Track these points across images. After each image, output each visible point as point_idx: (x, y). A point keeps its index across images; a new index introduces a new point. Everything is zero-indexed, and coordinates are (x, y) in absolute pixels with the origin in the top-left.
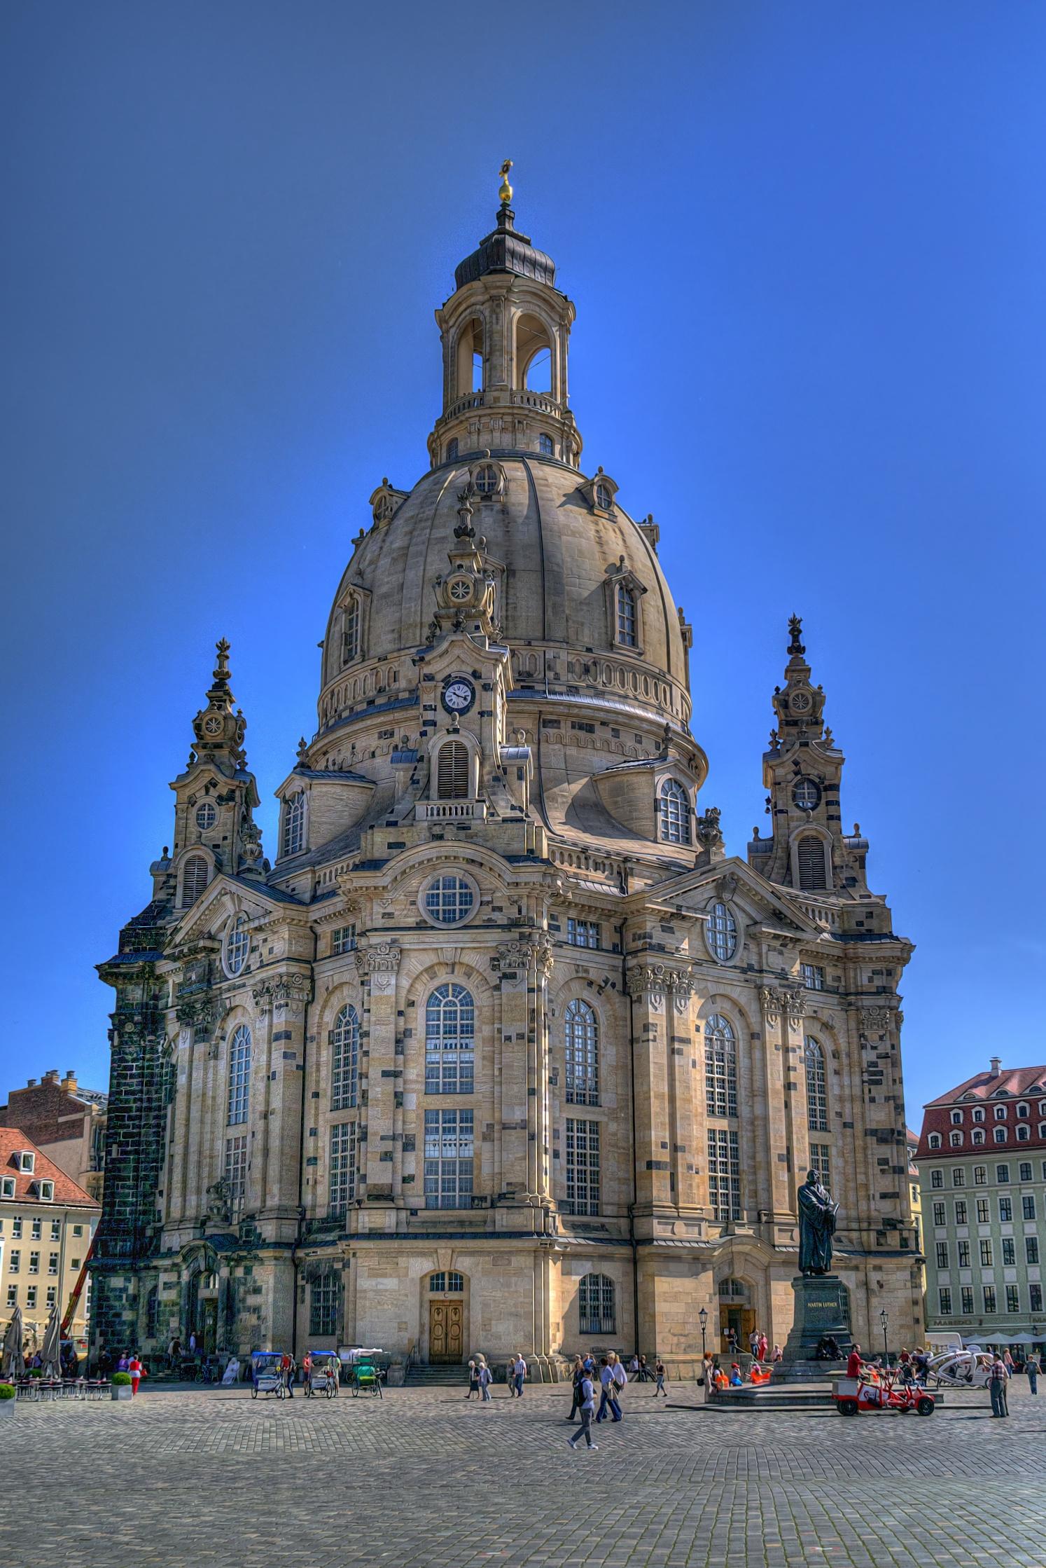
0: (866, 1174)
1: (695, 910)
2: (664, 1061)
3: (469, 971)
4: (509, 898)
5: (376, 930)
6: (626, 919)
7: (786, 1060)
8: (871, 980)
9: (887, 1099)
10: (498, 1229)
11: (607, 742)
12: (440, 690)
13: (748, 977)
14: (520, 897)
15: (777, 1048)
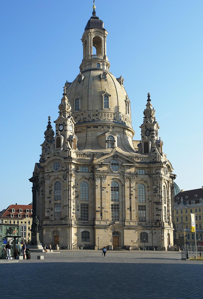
0: (154, 211)
1: (106, 163)
2: (100, 192)
3: (60, 179)
4: (65, 165)
5: (46, 173)
6: (93, 166)
7: (131, 189)
8: (155, 171)
9: (158, 196)
10: (63, 223)
11: (101, 129)
12: (58, 127)
13: (121, 174)
14: (67, 165)
15: (128, 187)
